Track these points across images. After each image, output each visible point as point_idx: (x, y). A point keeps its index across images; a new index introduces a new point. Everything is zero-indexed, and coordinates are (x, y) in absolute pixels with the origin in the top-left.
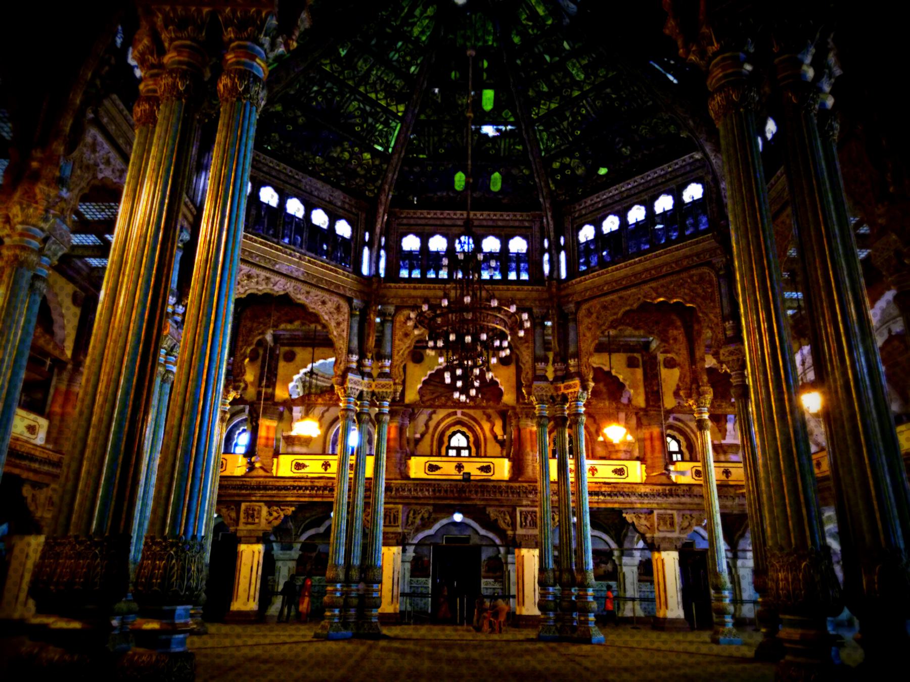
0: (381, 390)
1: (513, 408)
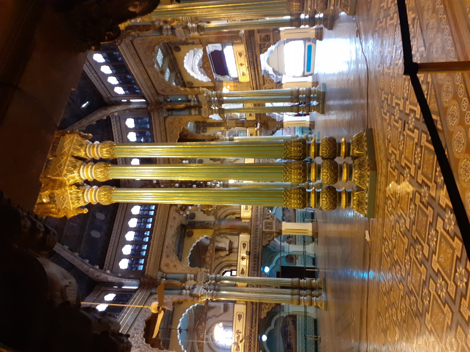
0: (203, 279)
1: (215, 230)
